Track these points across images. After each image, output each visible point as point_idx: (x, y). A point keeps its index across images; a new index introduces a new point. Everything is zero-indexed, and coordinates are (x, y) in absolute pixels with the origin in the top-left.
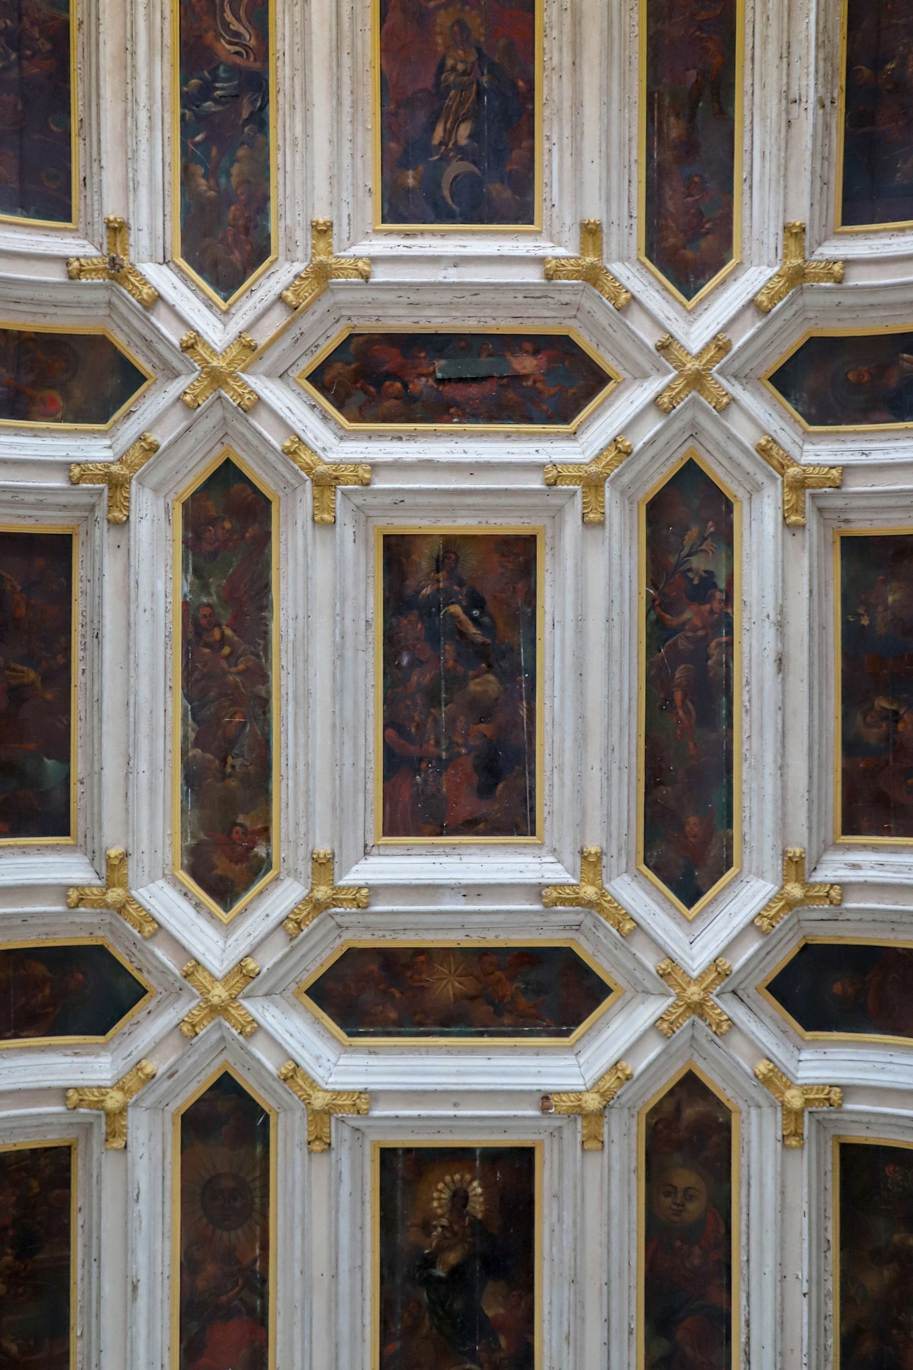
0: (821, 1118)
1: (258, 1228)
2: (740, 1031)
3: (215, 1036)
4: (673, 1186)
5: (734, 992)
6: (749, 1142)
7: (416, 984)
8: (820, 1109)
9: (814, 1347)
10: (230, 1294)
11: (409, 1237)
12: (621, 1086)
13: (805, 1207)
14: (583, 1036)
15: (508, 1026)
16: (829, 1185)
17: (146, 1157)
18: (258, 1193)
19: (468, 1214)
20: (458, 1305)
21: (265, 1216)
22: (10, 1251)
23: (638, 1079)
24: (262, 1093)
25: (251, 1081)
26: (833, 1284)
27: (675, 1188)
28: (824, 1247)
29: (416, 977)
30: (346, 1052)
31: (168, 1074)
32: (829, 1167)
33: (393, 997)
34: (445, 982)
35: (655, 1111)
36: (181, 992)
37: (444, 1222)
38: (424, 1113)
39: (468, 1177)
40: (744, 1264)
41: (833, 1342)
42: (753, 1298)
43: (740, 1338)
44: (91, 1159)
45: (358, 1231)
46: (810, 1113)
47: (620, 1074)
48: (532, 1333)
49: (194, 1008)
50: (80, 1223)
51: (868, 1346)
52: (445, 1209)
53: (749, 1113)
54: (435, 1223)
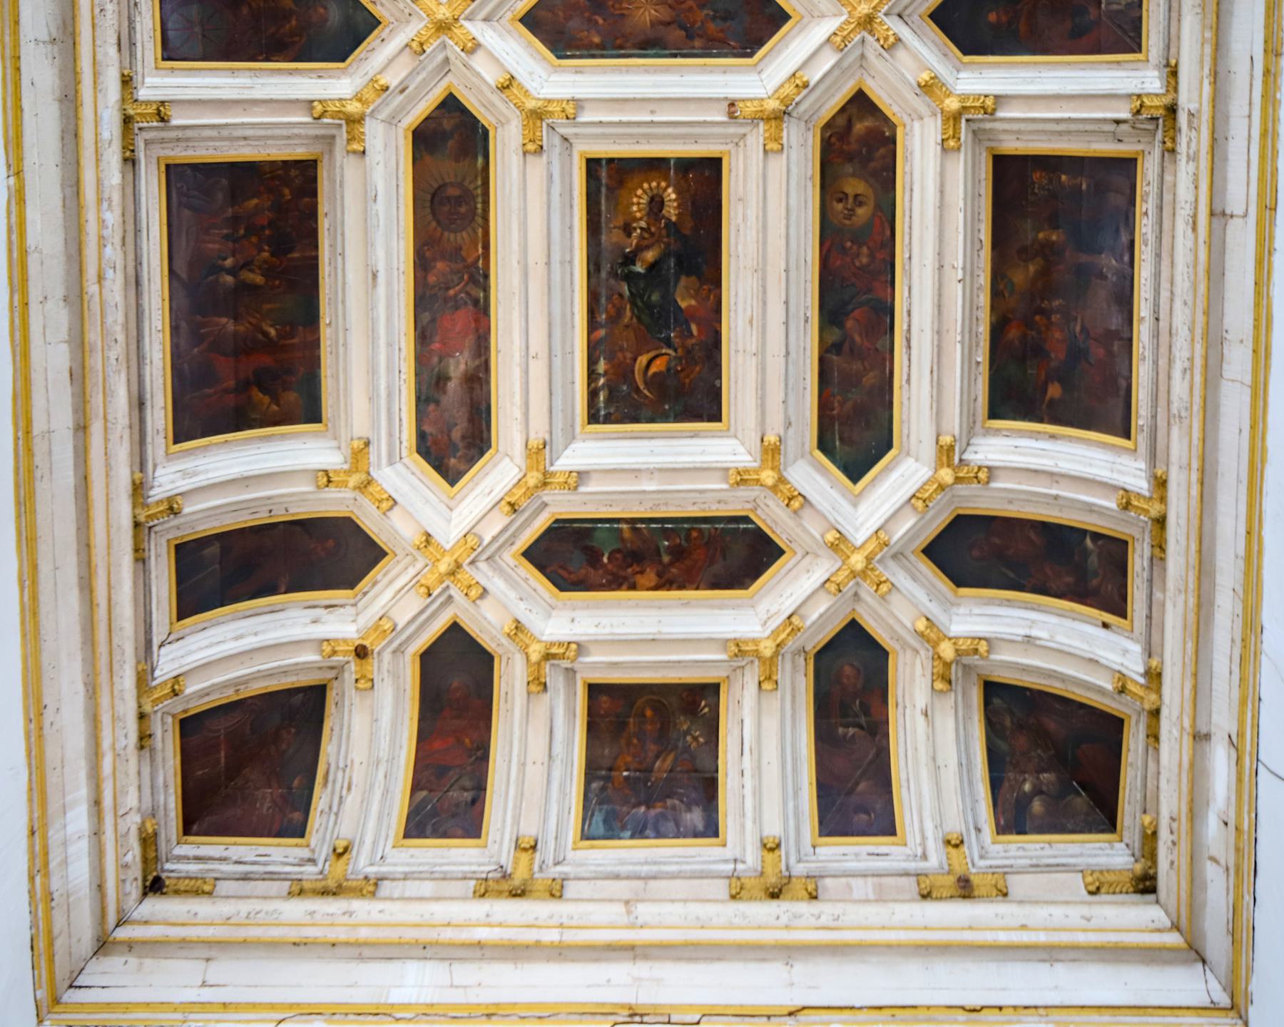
0: (976, 128)
1: (480, 231)
2: (905, 46)
3: (440, 57)
4: (843, 192)
5: (900, 16)
6: (911, 153)
7: (617, 12)
8: (975, 117)
9: (967, 330)
10: (457, 288)
11: (610, 238)
12: (799, 94)
13: (961, 204)
14: (765, 56)
15: (698, 49)
16: (983, 192)
17: (382, 165)
18: (480, 199)
19: (663, 217)
20: (655, 297)
21: (486, 219)
22: (266, 248)
23: (813, 89)
24: (482, 110)
25: (473, 99)
26: (984, 279)
27: (846, 195)
28: (977, 246)
29: (617, 6)
30: (556, 72)
31: (400, 88)
32: (983, 176)
33: (597, 22)
34: (642, 10)
35: (828, 126)
36: (411, 18)
37: (643, 224)
38: (625, 119)
39: (663, 184)
40: (906, 261)
41: (984, 329)
42: (915, 291)
43: (902, 327)
44: (334, 168)
45: (568, 231)
46: (968, 120)
47: (798, 82)
48: (720, 322)
49: (422, 29)
50: (326, 226)
51: (1013, 334)
52: (643, 212)
53: (912, 127)
54: (635, 225)
